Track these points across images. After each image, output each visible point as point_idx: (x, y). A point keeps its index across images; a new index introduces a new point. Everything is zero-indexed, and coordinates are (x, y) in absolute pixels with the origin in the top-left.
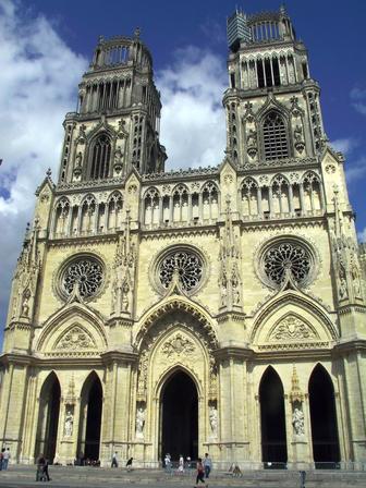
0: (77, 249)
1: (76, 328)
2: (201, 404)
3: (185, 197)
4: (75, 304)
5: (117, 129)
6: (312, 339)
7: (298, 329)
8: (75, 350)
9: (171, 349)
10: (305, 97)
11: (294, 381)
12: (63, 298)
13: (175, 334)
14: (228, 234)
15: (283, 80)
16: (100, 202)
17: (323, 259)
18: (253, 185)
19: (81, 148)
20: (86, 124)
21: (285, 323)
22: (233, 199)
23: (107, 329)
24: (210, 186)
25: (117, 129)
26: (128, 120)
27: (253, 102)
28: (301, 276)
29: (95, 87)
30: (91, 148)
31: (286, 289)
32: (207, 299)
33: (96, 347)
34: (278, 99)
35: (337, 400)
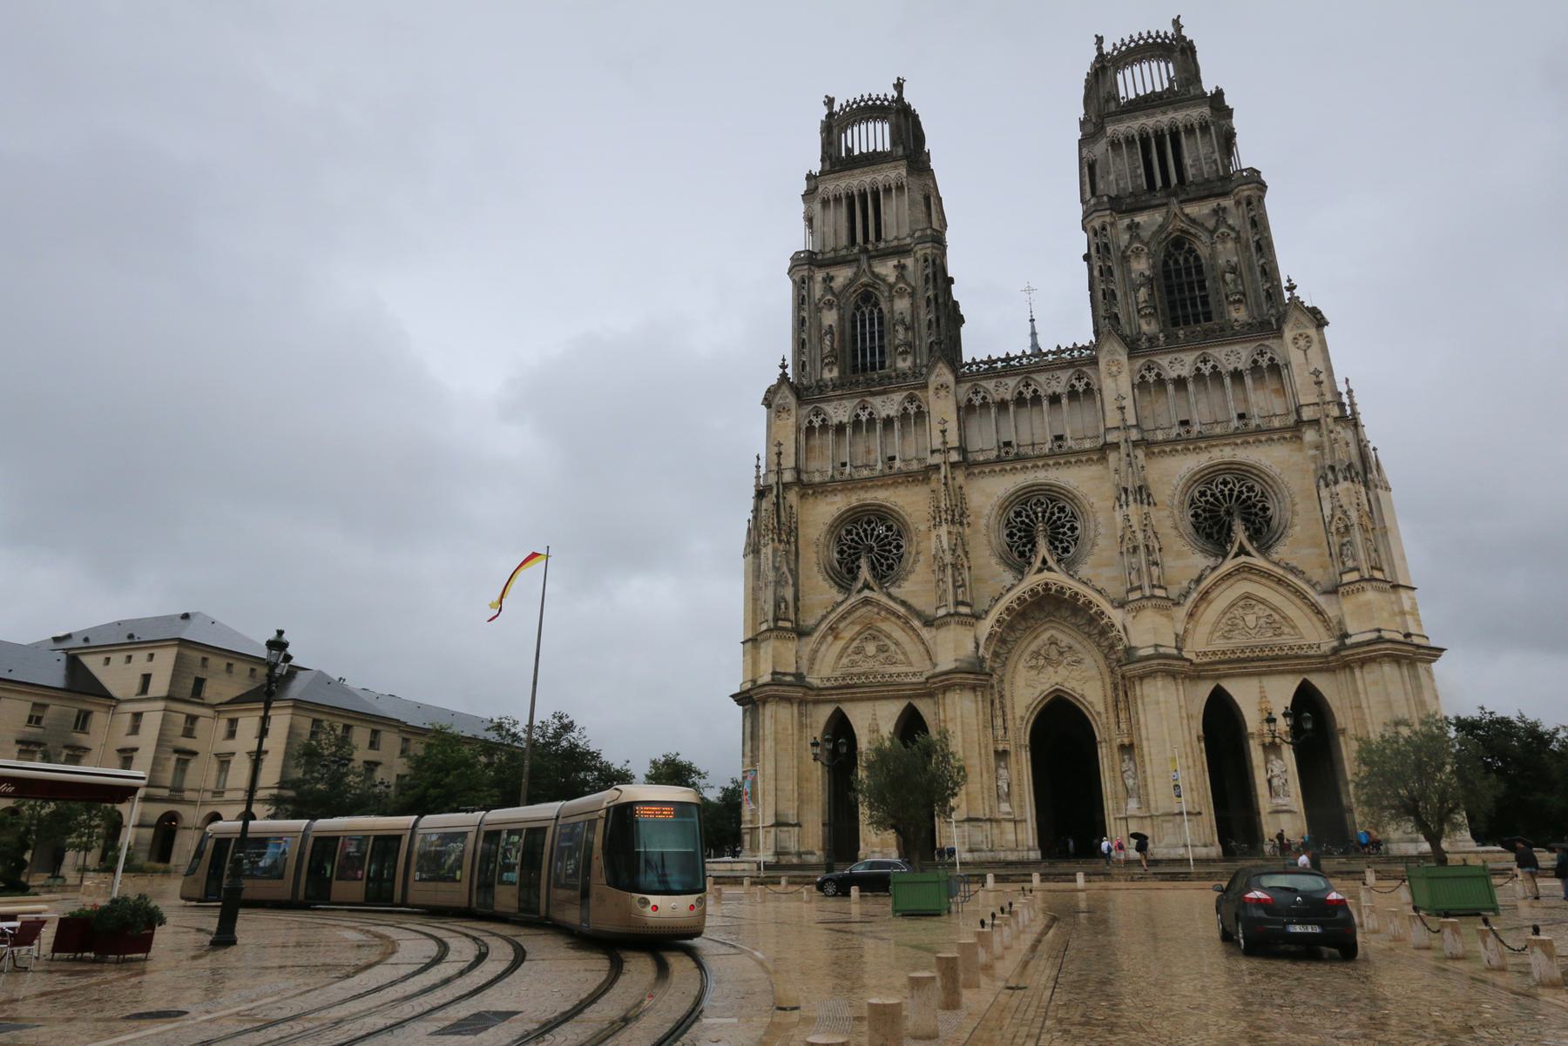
0: (854, 499)
1: (871, 632)
2: (1103, 752)
3: (1036, 399)
4: (866, 593)
5: (892, 279)
6: (1288, 639)
7: (1262, 621)
8: (870, 663)
9: (1042, 662)
10: (1238, 203)
12: (845, 588)
14: (1130, 464)
15: (1190, 173)
16: (884, 415)
17: (1297, 500)
18: (1158, 375)
19: (830, 318)
20: (833, 271)
21: (1238, 612)
24: (1079, 379)
25: (892, 279)
26: (909, 262)
27: (1140, 218)
29: (837, 199)
30: (848, 316)
31: (1236, 555)
33: (911, 664)
34: (1188, 210)
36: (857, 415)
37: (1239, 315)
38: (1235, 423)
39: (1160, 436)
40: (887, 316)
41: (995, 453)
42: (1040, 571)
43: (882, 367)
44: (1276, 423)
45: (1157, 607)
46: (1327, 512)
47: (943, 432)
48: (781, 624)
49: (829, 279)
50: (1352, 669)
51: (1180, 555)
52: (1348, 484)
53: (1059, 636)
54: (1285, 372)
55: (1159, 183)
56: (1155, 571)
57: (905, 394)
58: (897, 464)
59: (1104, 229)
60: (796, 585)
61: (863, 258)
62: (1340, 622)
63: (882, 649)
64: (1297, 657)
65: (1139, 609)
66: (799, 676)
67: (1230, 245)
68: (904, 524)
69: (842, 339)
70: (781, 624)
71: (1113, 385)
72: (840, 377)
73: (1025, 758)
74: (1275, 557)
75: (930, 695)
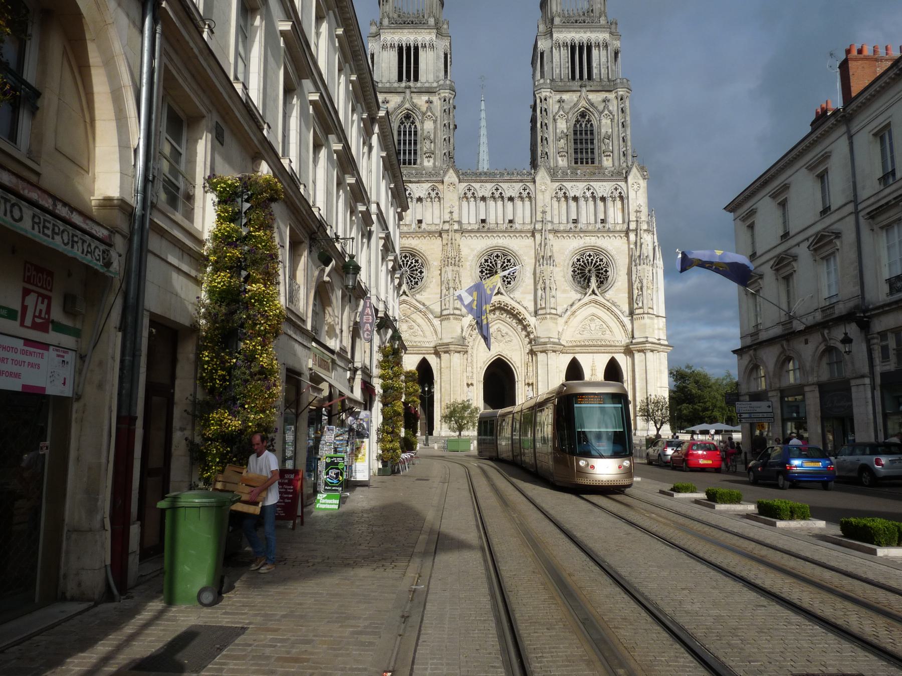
5: (424, 109)
6: (608, 336)
22: (548, 209)
23: (436, 322)
24: (525, 190)
25: (424, 109)
26: (435, 99)
27: (566, 96)
28: (602, 282)
32: (521, 297)
33: (425, 336)
37: (607, 163)
38: (599, 225)
39: (562, 228)
40: (419, 133)
44: (618, 228)
45: (551, 318)
47: (451, 213)
50: (633, 355)
51: (564, 291)
52: (645, 266)
53: (502, 328)
55: (577, 76)
57: (430, 184)
58: (423, 226)
59: (546, 99)
61: (408, 91)
63: (410, 328)
67: (609, 121)
71: (541, 197)
73: (481, 386)
74: (607, 295)
75: (437, 354)
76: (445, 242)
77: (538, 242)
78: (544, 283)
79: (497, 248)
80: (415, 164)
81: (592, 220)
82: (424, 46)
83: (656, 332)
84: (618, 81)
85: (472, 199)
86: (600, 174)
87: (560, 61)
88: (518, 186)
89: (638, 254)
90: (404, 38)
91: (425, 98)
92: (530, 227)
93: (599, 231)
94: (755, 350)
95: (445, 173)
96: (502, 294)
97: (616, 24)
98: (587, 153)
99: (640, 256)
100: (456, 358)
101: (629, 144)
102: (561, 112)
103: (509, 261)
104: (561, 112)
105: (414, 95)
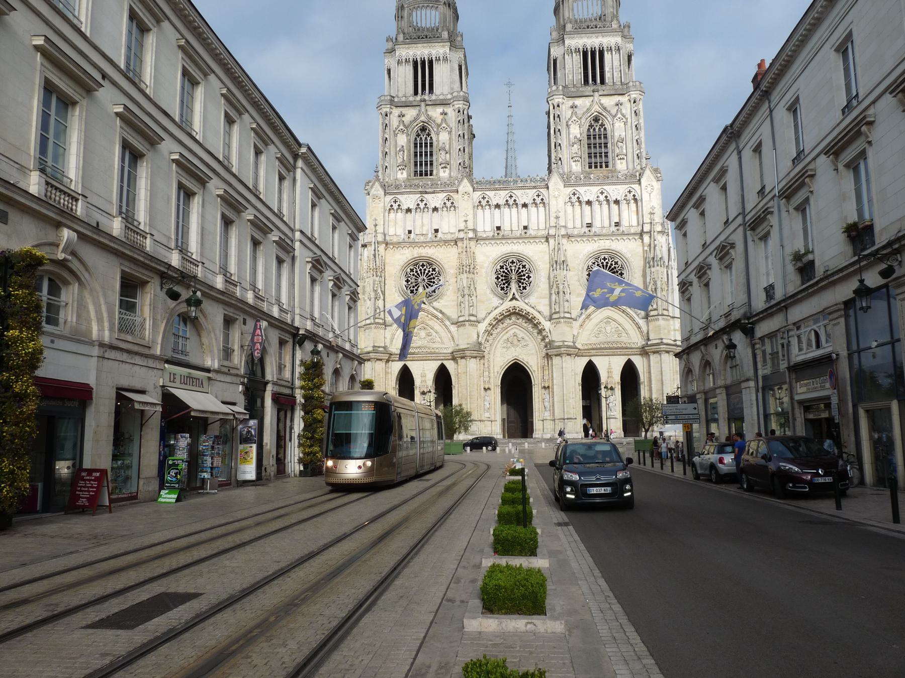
0: (417, 252)
5: (439, 121)
6: (624, 338)
9: (509, 345)
11: (609, 372)
13: (513, 331)
19: (402, 140)
20: (404, 110)
21: (603, 325)
22: (561, 214)
23: (453, 328)
24: (538, 196)
25: (439, 121)
27: (578, 102)
29: (407, 61)
33: (443, 343)
34: (602, 102)
35: (642, 386)
36: (418, 205)
37: (621, 166)
38: (613, 228)
39: (576, 232)
41: (491, 234)
42: (511, 300)
43: (431, 175)
44: (632, 231)
46: (648, 280)
48: (377, 321)
49: (402, 115)
52: (659, 268)
54: (640, 203)
56: (566, 304)
58: (439, 235)
59: (558, 106)
60: (384, 300)
61: (423, 104)
62: (648, 333)
64: (627, 348)
65: (557, 323)
66: (385, 347)
68: (442, 268)
69: (409, 155)
70: (377, 321)
71: (555, 202)
72: (408, 179)
73: (499, 390)
75: (454, 359)
76: (460, 250)
77: (552, 247)
78: (558, 288)
79: (511, 254)
80: (431, 175)
81: (606, 224)
82: (438, 60)
83: (672, 333)
84: (631, 84)
85: (487, 207)
86: (613, 178)
87: (572, 68)
88: (532, 193)
89: (652, 256)
90: (419, 53)
91: (440, 110)
92: (545, 233)
93: (613, 234)
94: (688, 354)
95: (460, 183)
96: (517, 299)
97: (629, 27)
98: (601, 156)
99: (653, 258)
100: (473, 364)
101: (643, 146)
102: (574, 118)
103: (524, 267)
104: (574, 118)
105: (429, 108)
